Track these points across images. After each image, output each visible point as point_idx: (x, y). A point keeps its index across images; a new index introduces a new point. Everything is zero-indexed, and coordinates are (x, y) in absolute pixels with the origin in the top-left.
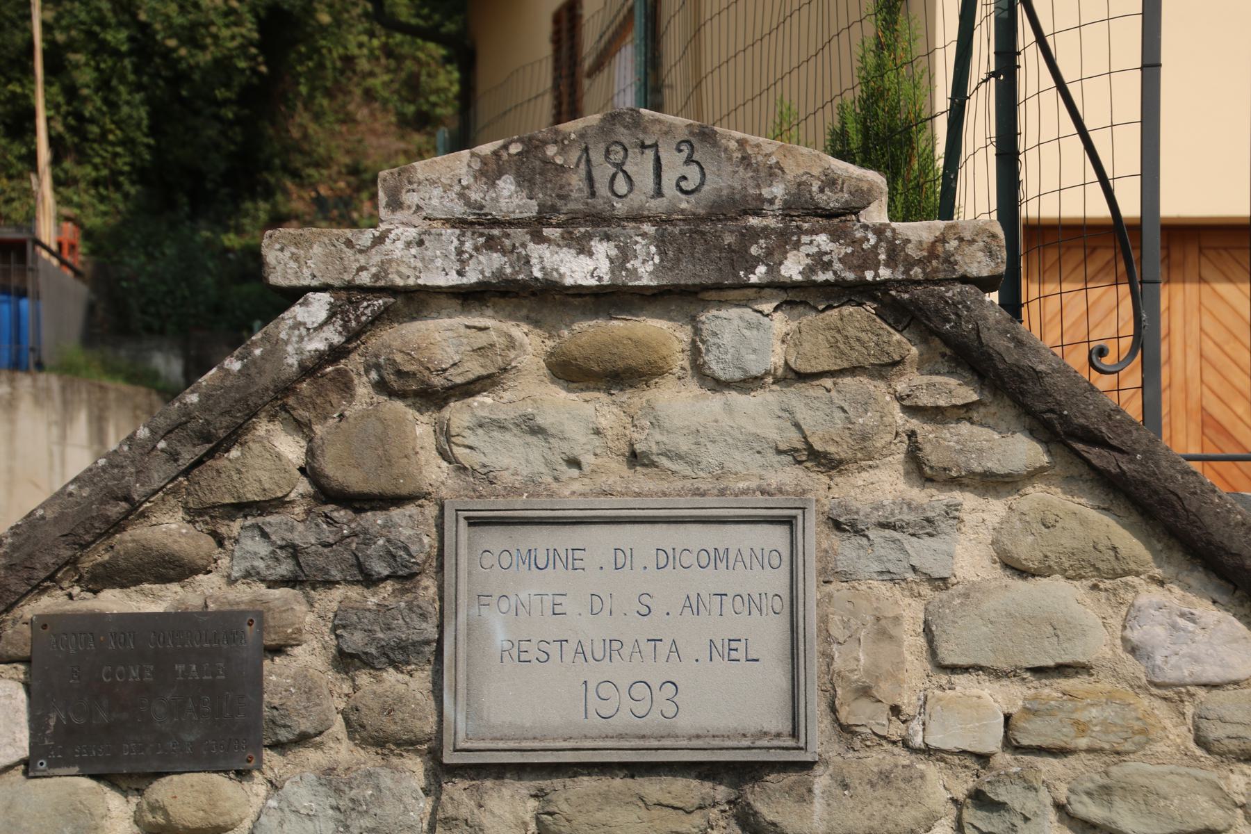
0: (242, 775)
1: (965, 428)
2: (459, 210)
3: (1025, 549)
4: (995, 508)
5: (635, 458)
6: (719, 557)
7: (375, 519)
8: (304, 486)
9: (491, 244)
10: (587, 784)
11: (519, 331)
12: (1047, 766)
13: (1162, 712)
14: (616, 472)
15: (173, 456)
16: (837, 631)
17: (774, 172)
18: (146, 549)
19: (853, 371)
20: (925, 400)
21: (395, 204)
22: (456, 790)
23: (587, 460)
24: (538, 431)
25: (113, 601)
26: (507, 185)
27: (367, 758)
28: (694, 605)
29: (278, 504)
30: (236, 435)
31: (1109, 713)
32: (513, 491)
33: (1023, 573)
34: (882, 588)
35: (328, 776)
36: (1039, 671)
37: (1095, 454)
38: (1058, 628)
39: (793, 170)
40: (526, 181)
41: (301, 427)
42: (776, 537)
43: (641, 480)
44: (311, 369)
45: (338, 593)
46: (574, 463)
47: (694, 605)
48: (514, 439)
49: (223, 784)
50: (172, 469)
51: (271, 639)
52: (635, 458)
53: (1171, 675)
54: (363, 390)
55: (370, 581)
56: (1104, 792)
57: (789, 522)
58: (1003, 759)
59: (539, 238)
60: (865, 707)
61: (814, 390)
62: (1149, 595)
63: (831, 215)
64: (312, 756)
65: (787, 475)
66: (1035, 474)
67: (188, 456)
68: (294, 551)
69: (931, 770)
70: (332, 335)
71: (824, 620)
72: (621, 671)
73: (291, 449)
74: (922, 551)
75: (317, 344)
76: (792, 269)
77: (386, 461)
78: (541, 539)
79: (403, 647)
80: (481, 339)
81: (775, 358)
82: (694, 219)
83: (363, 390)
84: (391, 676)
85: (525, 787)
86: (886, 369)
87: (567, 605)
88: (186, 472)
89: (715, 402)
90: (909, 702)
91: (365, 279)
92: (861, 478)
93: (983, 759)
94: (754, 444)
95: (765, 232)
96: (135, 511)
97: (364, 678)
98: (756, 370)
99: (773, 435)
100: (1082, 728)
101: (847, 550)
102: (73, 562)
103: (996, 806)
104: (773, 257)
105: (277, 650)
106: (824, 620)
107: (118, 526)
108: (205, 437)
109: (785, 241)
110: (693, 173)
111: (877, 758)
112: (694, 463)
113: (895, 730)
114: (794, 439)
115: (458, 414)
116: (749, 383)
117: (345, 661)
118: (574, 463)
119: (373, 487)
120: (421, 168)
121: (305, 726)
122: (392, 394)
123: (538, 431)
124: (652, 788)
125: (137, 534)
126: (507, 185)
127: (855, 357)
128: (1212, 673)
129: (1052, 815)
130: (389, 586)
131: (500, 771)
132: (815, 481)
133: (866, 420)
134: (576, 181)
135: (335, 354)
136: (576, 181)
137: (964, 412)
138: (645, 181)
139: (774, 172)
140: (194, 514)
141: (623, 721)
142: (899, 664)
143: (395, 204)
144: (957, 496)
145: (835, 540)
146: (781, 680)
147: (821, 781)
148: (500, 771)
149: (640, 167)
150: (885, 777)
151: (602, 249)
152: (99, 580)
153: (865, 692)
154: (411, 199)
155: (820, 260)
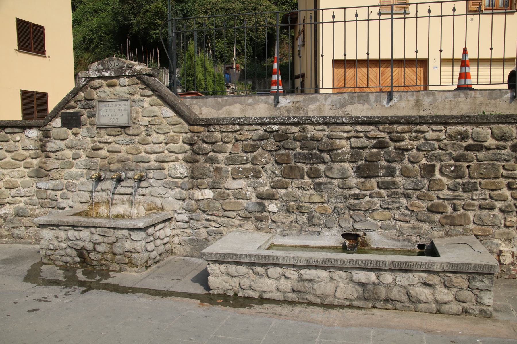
0: (80, 128)
1: (145, 90)
2: (96, 69)
3: (151, 103)
4: (149, 99)
5: (114, 95)
6: (122, 105)
7: (90, 102)
8: (84, 99)
9: (99, 72)
10: (110, 129)
11: (103, 81)
12: (153, 126)
13: (164, 120)
14: (113, 96)
15: (72, 96)
16: (132, 113)
17: (125, 63)
18: (70, 105)
19: (134, 84)
20: (141, 87)
21: (90, 68)
22: (98, 129)
23: (110, 95)
24: (105, 92)
25: (68, 111)
26: (100, 66)
27: (90, 126)
28: (119, 110)
29: (81, 100)
30: (77, 94)
31: (159, 121)
32: (103, 98)
33: (152, 106)
34: (137, 108)
35: (87, 129)
36: (152, 116)
37: (156, 93)
38: (153, 112)
39: (127, 63)
40: (102, 65)
41: (83, 92)
42: (126, 103)
43: (115, 97)
44: (84, 86)
45: (88, 109)
46: (108, 95)
47: (119, 110)
48: (103, 93)
49: (78, 129)
50: (71, 97)
51: (81, 114)
52: (114, 95)
53: (165, 116)
54: (89, 88)
55: (90, 108)
56: (158, 129)
57: (127, 101)
58: (149, 126)
59: (103, 71)
60: (135, 120)
61: (130, 87)
62: (163, 108)
63: (131, 67)
64: (86, 126)
65: (128, 96)
66: (152, 95)
67: (73, 96)
68: (83, 105)
69: (142, 127)
70: (85, 83)
71: (131, 111)
73: (83, 95)
74: (141, 104)
75: (84, 84)
76: (127, 74)
77: (91, 96)
78: (105, 103)
79: (93, 115)
80: (99, 82)
81: (127, 83)
82: (117, 68)
83: (89, 88)
84: (93, 118)
85: (104, 129)
86: (137, 84)
87: (108, 110)
88: (73, 97)
89: (122, 88)
90: (139, 120)
91: (87, 76)
92: (135, 96)
93: (147, 126)
94: (125, 92)
95: (124, 70)
96: (69, 102)
97: (90, 118)
98: (125, 85)
99: (127, 92)
100: (156, 122)
101: (134, 104)
102: (64, 107)
103: (148, 131)
104: (125, 72)
105: (82, 116)
106: (131, 111)
107: (68, 103)
108: (74, 94)
109: (126, 71)
110: (117, 63)
111: (137, 126)
113: (139, 123)
114: (128, 92)
115: (98, 90)
116: (125, 86)
117: (89, 117)
118: (108, 95)
119: (90, 98)
120: (92, 64)
121: (84, 123)
122: (92, 89)
123: (105, 92)
124: (116, 129)
125: (70, 104)
126: (100, 66)
127: (134, 83)
128: (168, 116)
129: (154, 132)
130: (92, 109)
131: (102, 128)
132: (131, 97)
133: (135, 90)
134: (107, 65)
135: (86, 84)
136: (107, 65)
137: (145, 89)
138: (113, 65)
139: (125, 63)
140: (75, 101)
141: (113, 122)
142: (139, 116)
143: (90, 68)
144: (145, 98)
145: (132, 103)
146: (127, 118)
147: (131, 128)
148: (102, 128)
149: (112, 63)
151: (109, 72)
152: (67, 109)
153: (135, 119)
154: (92, 68)
155: (129, 73)
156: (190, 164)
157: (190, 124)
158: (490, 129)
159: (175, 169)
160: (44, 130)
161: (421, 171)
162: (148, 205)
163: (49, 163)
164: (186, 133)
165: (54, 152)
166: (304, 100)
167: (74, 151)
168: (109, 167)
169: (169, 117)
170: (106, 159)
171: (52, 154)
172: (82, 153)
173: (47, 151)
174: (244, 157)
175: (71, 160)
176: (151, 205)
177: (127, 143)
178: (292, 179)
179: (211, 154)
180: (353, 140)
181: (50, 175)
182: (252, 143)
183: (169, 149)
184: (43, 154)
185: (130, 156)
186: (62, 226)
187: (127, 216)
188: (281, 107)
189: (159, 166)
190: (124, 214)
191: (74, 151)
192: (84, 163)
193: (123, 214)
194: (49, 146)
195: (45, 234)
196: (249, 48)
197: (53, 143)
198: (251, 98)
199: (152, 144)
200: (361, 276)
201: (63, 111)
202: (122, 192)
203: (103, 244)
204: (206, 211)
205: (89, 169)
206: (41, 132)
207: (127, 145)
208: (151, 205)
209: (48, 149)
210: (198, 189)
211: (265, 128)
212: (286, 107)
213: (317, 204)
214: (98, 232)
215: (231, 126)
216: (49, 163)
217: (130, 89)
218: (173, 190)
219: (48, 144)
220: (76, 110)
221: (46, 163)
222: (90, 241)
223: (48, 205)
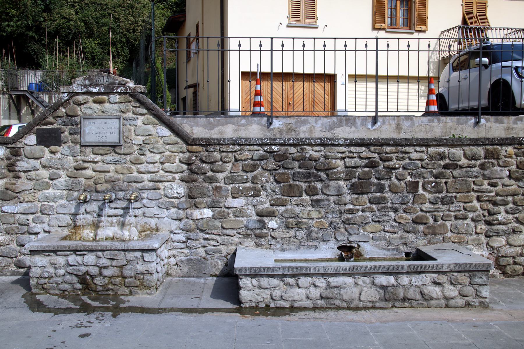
0: (60, 146)
1: (139, 108)
2: (82, 84)
3: (145, 122)
4: (142, 117)
5: (102, 112)
6: (111, 123)
7: (73, 118)
8: (65, 115)
9: (85, 88)
10: (97, 148)
11: (89, 97)
12: (147, 145)
13: (160, 139)
14: (100, 113)
15: (50, 111)
16: (124, 131)
17: (117, 80)
18: (48, 121)
19: (126, 102)
20: (134, 105)
21: (74, 83)
22: (83, 148)
23: (97, 112)
24: (91, 109)
25: (45, 127)
26: (87, 81)
27: (73, 145)
28: (108, 128)
29: (62, 117)
30: (57, 109)
31: (154, 140)
32: (89, 115)
33: (145, 124)
34: (129, 126)
35: (69, 147)
36: (147, 135)
37: (152, 112)
38: (148, 130)
39: (119, 80)
40: (89, 80)
41: (65, 108)
42: (118, 120)
43: (103, 114)
44: (66, 101)
45: (70, 126)
46: (95, 112)
47: (108, 128)
48: (89, 109)
49: (57, 147)
50: (50, 113)
51: (62, 131)
52: (102, 112)
53: (160, 136)
54: (72, 104)
55: (73, 125)
56: (153, 148)
57: (119, 119)
58: (143, 145)
59: (90, 87)
60: (127, 139)
61: (122, 104)
62: (159, 127)
63: (123, 84)
64: (67, 144)
65: (119, 114)
66: (146, 114)
67: (52, 111)
68: (64, 122)
69: (135, 146)
70: (68, 98)
71: (123, 130)
72: (101, 135)
73: (64, 110)
74: (134, 122)
75: (66, 99)
76: (119, 91)
77: (74, 112)
78: (92, 121)
79: (76, 132)
80: (85, 98)
81: (118, 100)
82: (108, 85)
83: (72, 104)
84: (76, 136)
85: (90, 148)
86: (130, 102)
87: (95, 128)
88: (52, 113)
89: (111, 105)
90: (132, 139)
91: (71, 91)
92: (127, 114)
93: (141, 145)
94: (115, 110)
95: (116, 86)
96: (46, 117)
97: (73, 136)
98: (115, 102)
99: (117, 109)
100: (151, 141)
101: (125, 122)
102: (40, 123)
103: (142, 150)
104: (117, 89)
105: (63, 133)
106: (123, 130)
107: (45, 119)
108: (54, 109)
109: (118, 87)
110: (108, 79)
111: (129, 145)
112: (109, 112)
113: (131, 142)
114: (120, 109)
115: (82, 107)
116: (115, 103)
117: (71, 134)
118: (95, 112)
119: (73, 115)
120: (77, 79)
121: (66, 141)
122: (75, 104)
123: (91, 109)
124: (104, 148)
125: (47, 120)
126: (87, 81)
127: (126, 100)
128: (165, 135)
129: (148, 151)
130: (75, 126)
131: (88, 146)
132: (122, 114)
133: (128, 107)
134: (95, 80)
135: (68, 100)
136: (95, 80)
137: (139, 107)
138: (103, 80)
139: (117, 80)
140: (53, 117)
141: (101, 141)
142: (131, 134)
143: (74, 83)
144: (138, 116)
145: (124, 121)
146: (118, 136)
147: (123, 147)
148: (88, 146)
149: (102, 79)
150: (130, 147)
151: (97, 88)
152: (43, 125)
153: (127, 138)
154: (76, 82)
155: (122, 90)
156: (187, 184)
157: (187, 144)
158: (463, 150)
159: (171, 189)
160: (13, 148)
161: (407, 187)
162: (141, 226)
163: (19, 184)
164: (183, 152)
165: (25, 172)
166: (296, 123)
167: (51, 171)
168: (96, 188)
169: (165, 137)
170: (92, 179)
171: (22, 175)
172: (61, 172)
173: (16, 171)
174: (244, 176)
175: (47, 180)
176: (145, 226)
177: (117, 163)
178: (291, 197)
179: (210, 173)
180: (347, 160)
181: (20, 197)
182: (252, 162)
183: (165, 168)
184: (11, 174)
185: (120, 176)
186: (61, 251)
187: (117, 239)
188: (274, 128)
189: (153, 186)
190: (113, 237)
191: (51, 171)
192: (64, 183)
193: (112, 236)
194: (19, 165)
195: (38, 261)
196: (125, 51)
197: (25, 162)
198: (244, 119)
199: (146, 164)
200: (382, 280)
201: (38, 127)
202: (110, 214)
203: (110, 267)
204: (205, 231)
205: (70, 190)
206: (8, 150)
207: (116, 164)
208: (145, 226)
209: (17, 169)
210: (196, 209)
211: (265, 149)
212: (278, 128)
213: (315, 219)
214: (106, 255)
215: (231, 146)
216: (19, 184)
217: (121, 107)
218: (169, 211)
219: (18, 163)
220: (55, 126)
221: (15, 184)
222: (96, 265)
223: (16, 231)
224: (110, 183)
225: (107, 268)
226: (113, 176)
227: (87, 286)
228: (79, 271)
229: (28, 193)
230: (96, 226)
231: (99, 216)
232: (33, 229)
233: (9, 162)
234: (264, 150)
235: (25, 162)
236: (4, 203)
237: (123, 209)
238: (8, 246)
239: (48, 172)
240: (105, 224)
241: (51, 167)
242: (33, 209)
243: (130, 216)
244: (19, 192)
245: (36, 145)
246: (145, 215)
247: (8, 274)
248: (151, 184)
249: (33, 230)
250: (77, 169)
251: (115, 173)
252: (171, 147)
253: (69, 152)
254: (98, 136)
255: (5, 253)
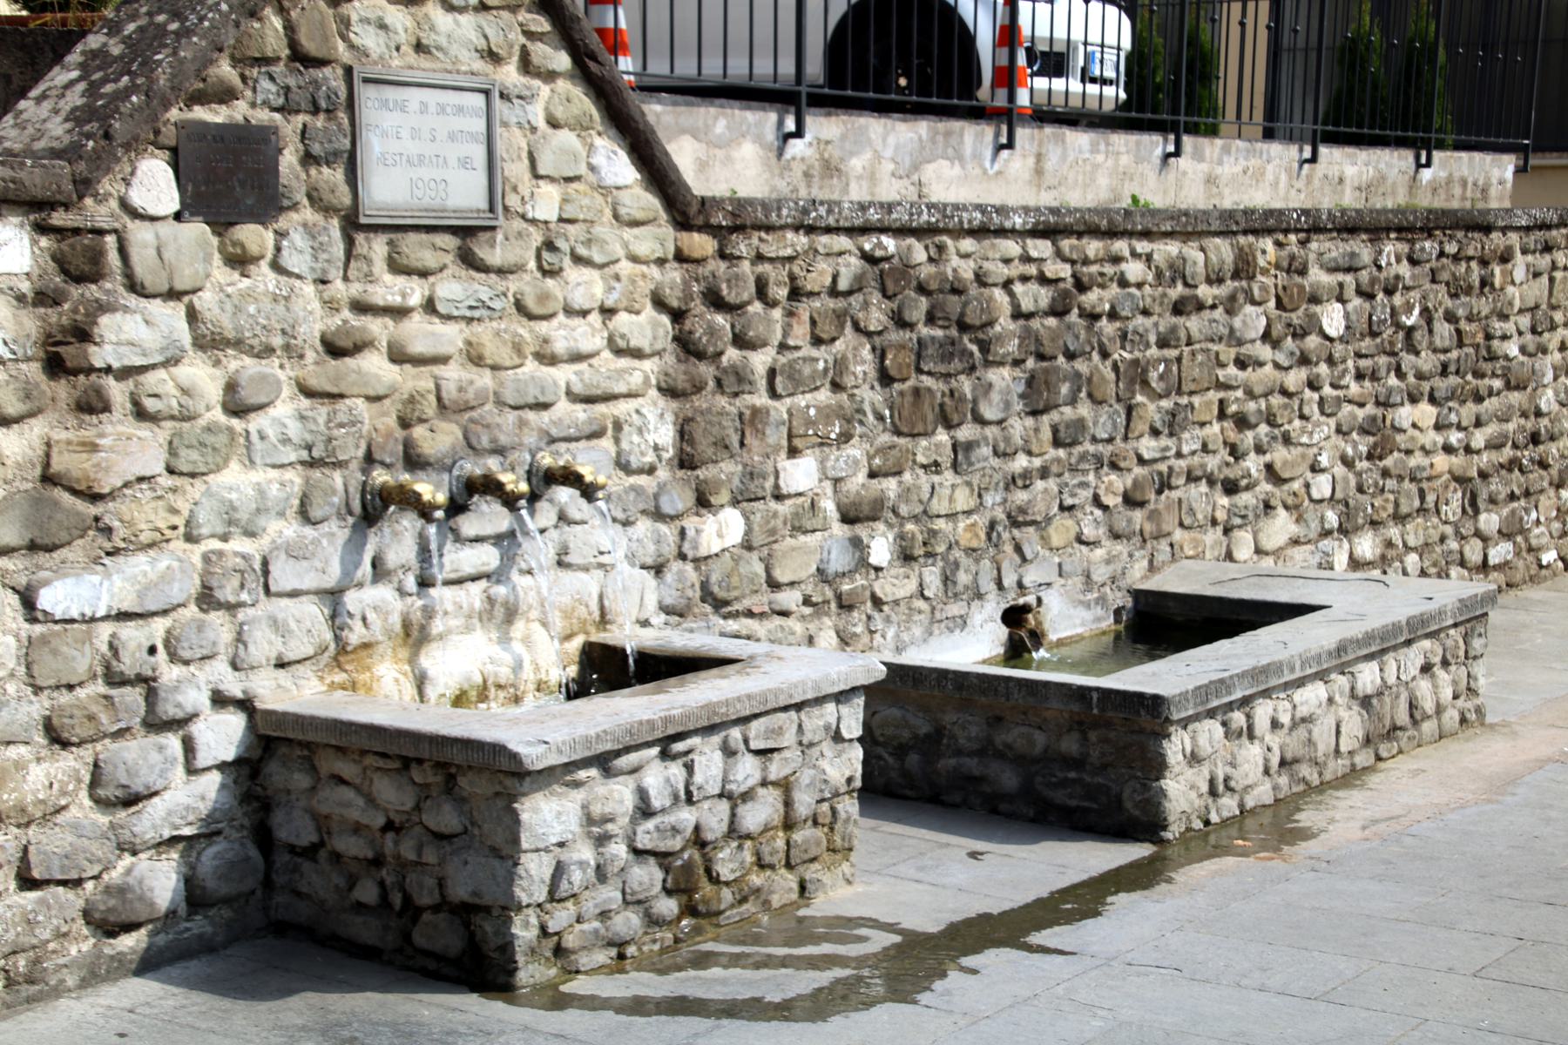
3: (560, 113)
28: (452, 137)
43: (423, 62)
47: (452, 137)
72: (425, 173)
78: (391, 93)
84: (325, 170)
112: (446, 54)
114: (482, 44)
140: (236, 61)
141: (426, 202)
150: (520, 234)
156: (674, 405)
157: (683, 222)
158: (1202, 249)
159: (640, 431)
160: (76, 231)
161: (1118, 379)
162: (567, 614)
163: (112, 450)
164: (661, 262)
165: (126, 373)
166: (844, 137)
167: (233, 365)
168: (408, 445)
169: (618, 188)
170: (387, 402)
171: (117, 392)
172: (279, 371)
173: (91, 370)
174: (817, 360)
175: (218, 415)
176: (573, 609)
177: (476, 314)
178: (913, 436)
179: (732, 354)
180: (1018, 288)
181: (116, 524)
182: (832, 303)
183: (623, 336)
184: (62, 390)
185: (485, 379)
186: (628, 750)
187: (499, 687)
188: (794, 159)
189: (590, 421)
190: (485, 681)
191: (233, 365)
192: (294, 430)
193: (479, 680)
194: (110, 336)
195: (549, 817)
197: (138, 317)
198: (724, 115)
199: (561, 317)
200: (1368, 676)
202: (468, 570)
203: (761, 791)
204: (727, 603)
205: (312, 463)
206: (44, 242)
207: (470, 320)
208: (573, 609)
209: (100, 356)
210: (704, 511)
211: (867, 247)
212: (803, 159)
213: (960, 517)
214: (757, 737)
215: (790, 235)
216: (112, 450)
217: (490, 32)
218: (630, 530)
219: (105, 320)
220: (238, 111)
221: (93, 448)
222: (721, 796)
223: (104, 718)
224: (457, 417)
225: (752, 799)
226: (471, 382)
227: (690, 899)
228: (675, 830)
229: (149, 494)
230: (415, 635)
231: (424, 583)
232: (180, 698)
233: (54, 319)
234: (861, 250)
235: (138, 317)
236: (40, 567)
237: (497, 539)
238: (60, 819)
239: (217, 372)
240: (454, 623)
241: (238, 344)
242: (176, 586)
243: (522, 572)
244: (112, 495)
245: (171, 221)
246: (567, 559)
247: (71, 981)
248: (580, 413)
249: (179, 705)
250: (334, 349)
251: (470, 366)
252: (636, 237)
253: (308, 258)
254: (416, 173)
255: (56, 862)
